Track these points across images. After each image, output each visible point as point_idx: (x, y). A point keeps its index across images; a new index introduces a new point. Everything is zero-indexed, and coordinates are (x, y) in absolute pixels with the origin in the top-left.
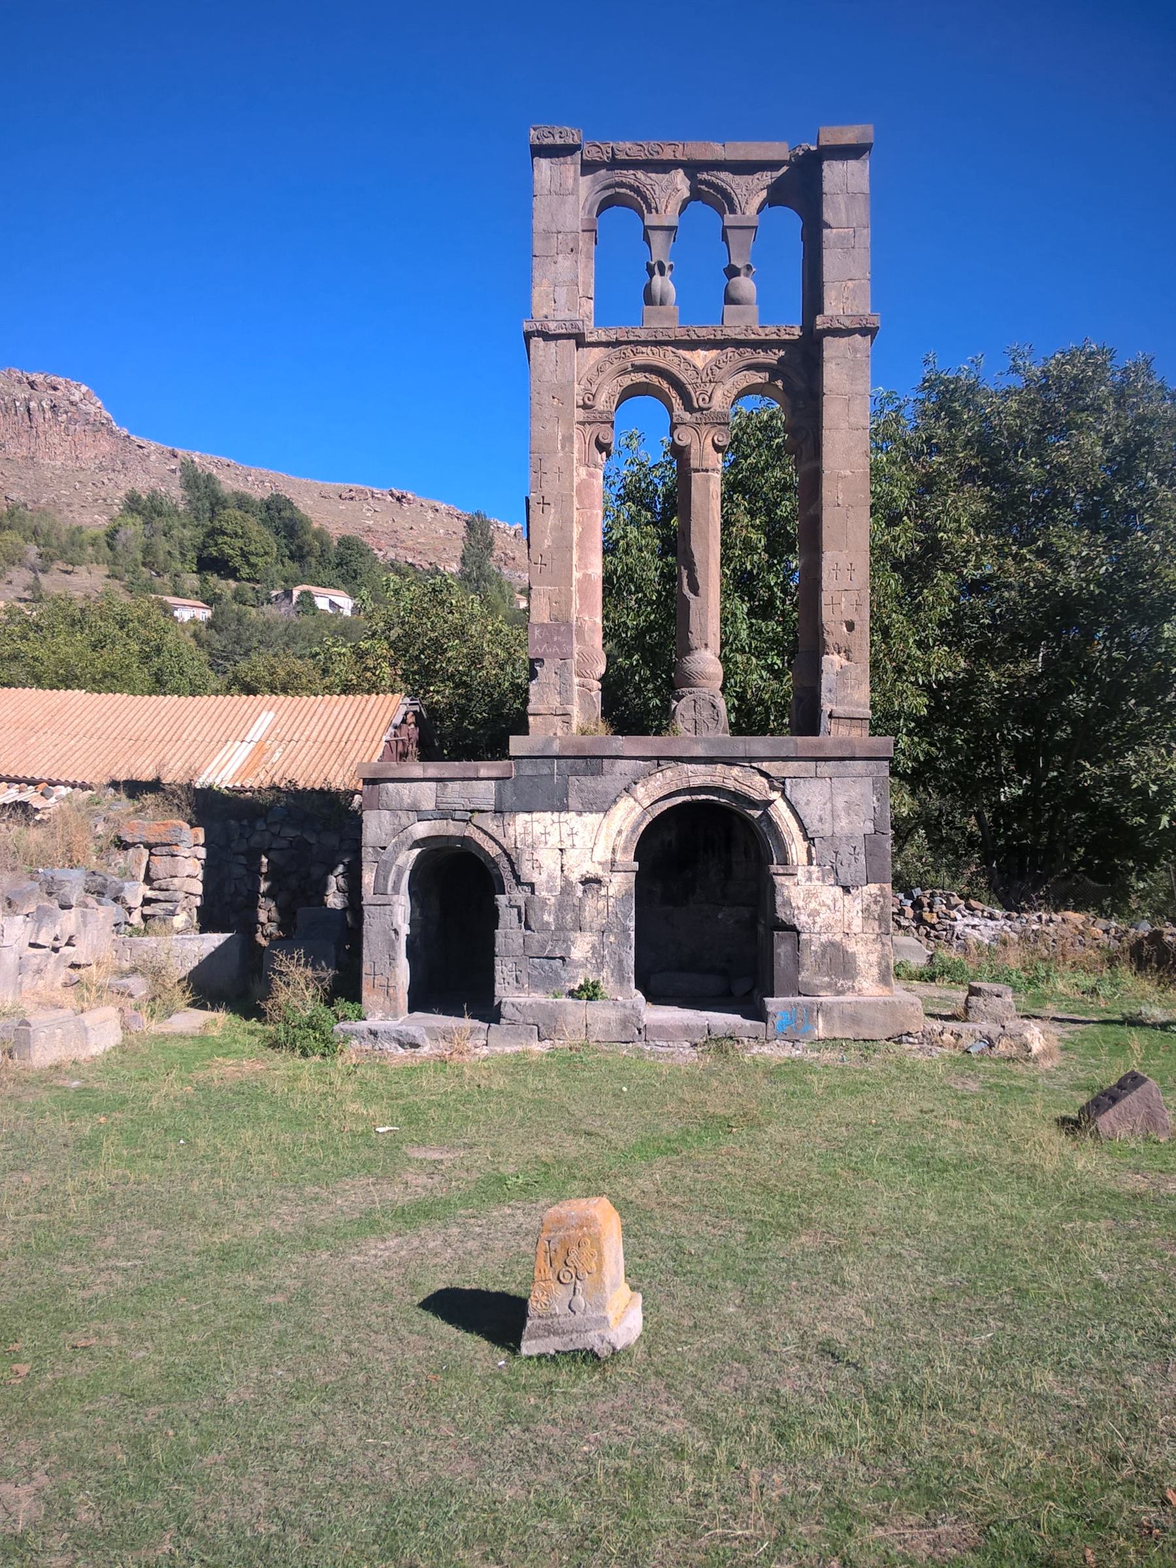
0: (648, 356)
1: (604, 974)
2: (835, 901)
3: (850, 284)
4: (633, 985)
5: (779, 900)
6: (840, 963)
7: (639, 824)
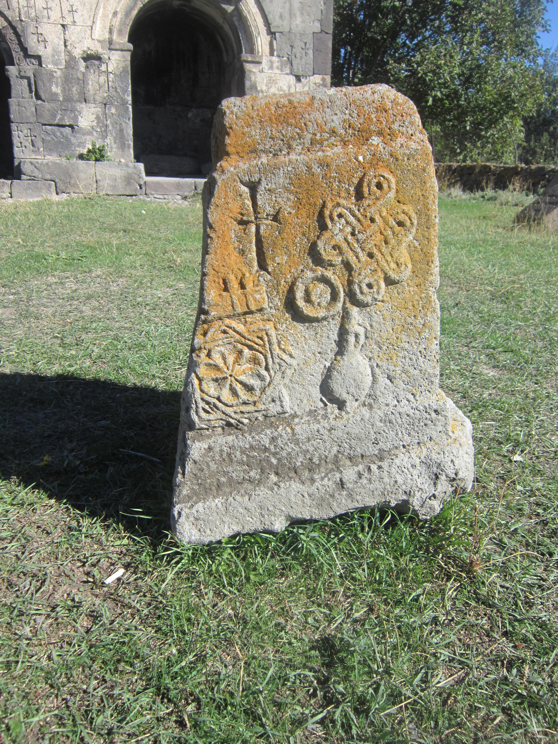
1: (108, 141)
2: (289, 87)
4: (132, 151)
5: (247, 84)
7: (132, 9)
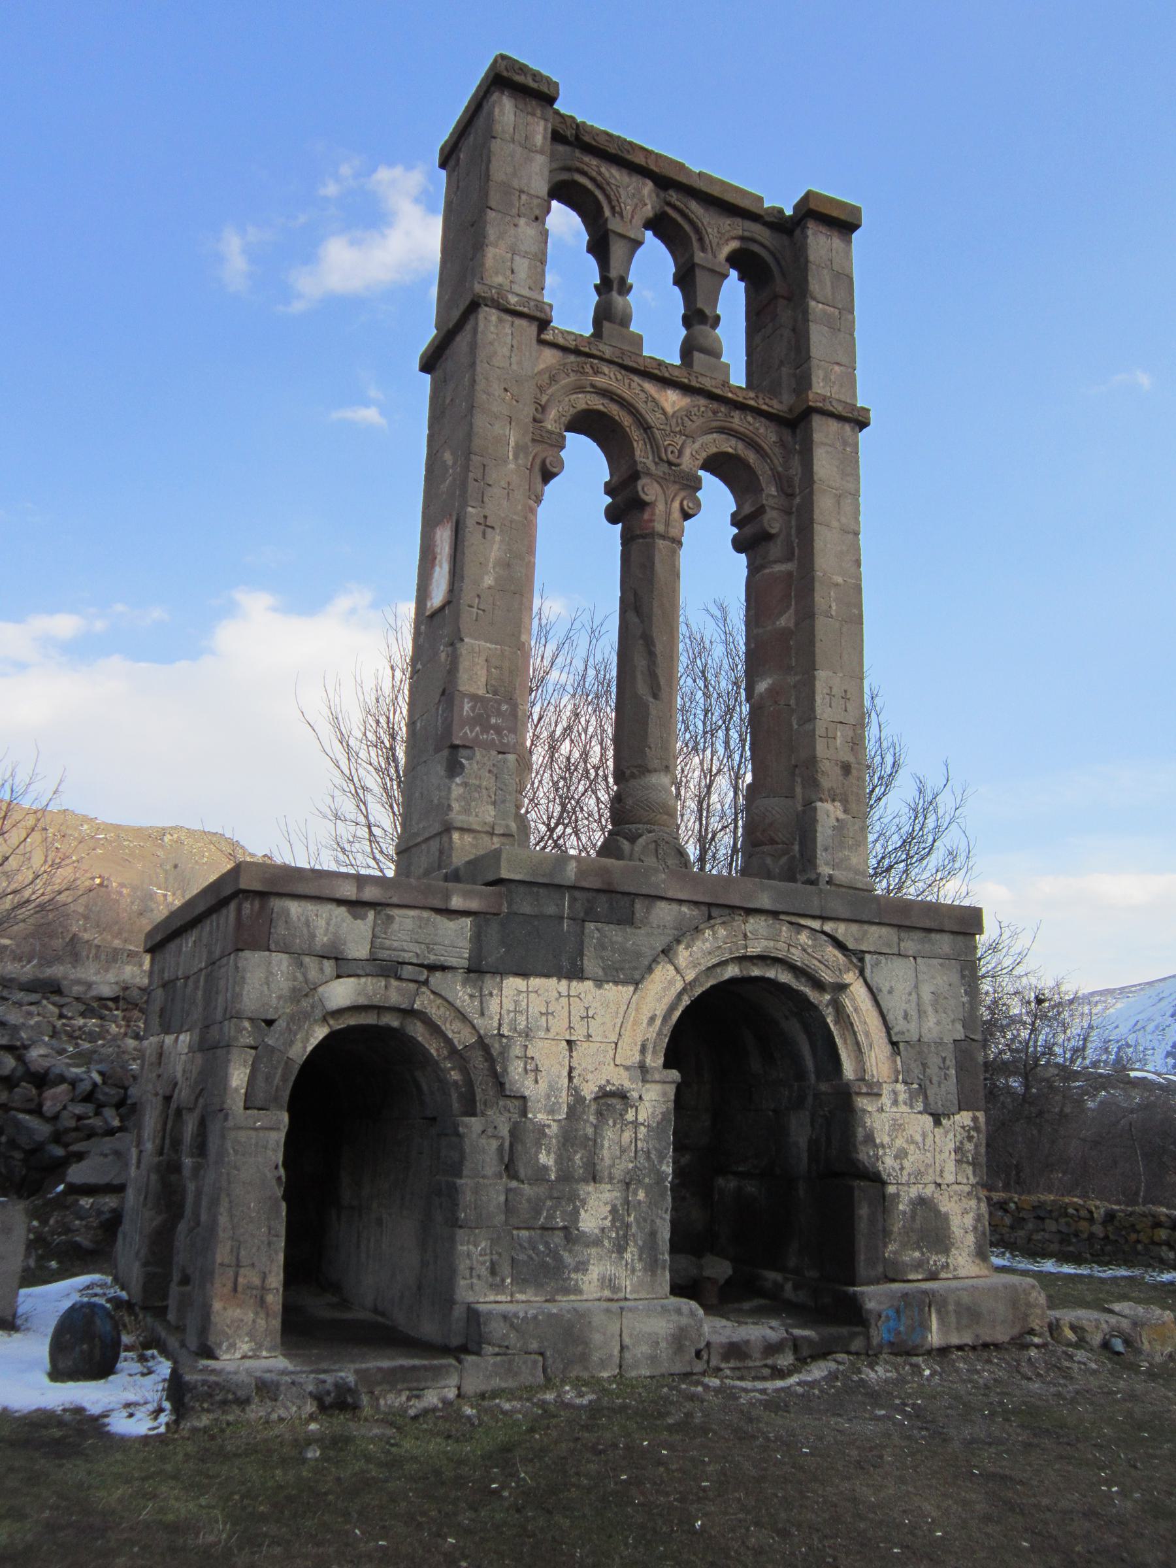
0: (609, 378)
2: (924, 1135)
3: (837, 368)
6: (932, 1230)
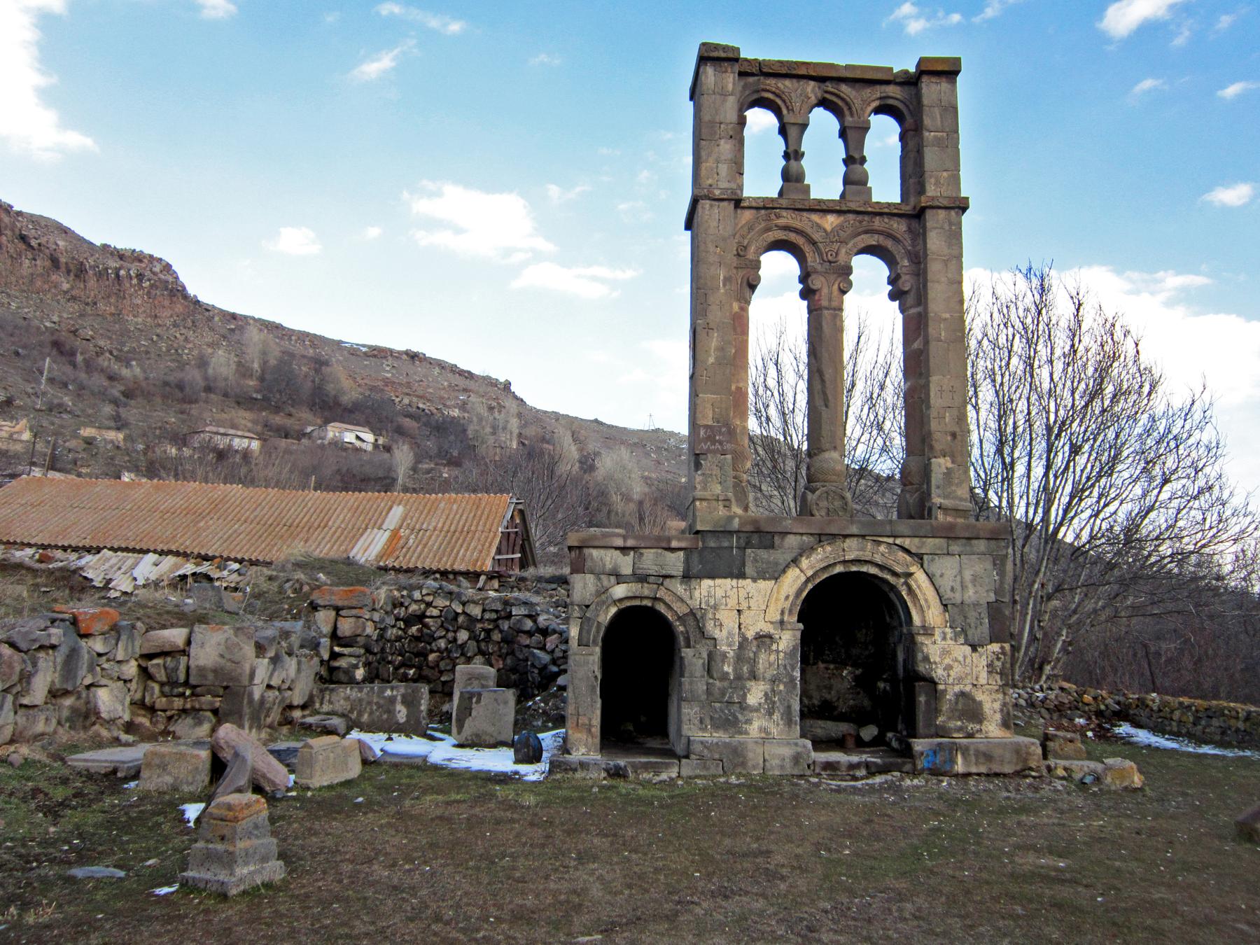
0: (787, 218)
2: (965, 657)
3: (945, 174)
5: (920, 656)
6: (970, 710)
